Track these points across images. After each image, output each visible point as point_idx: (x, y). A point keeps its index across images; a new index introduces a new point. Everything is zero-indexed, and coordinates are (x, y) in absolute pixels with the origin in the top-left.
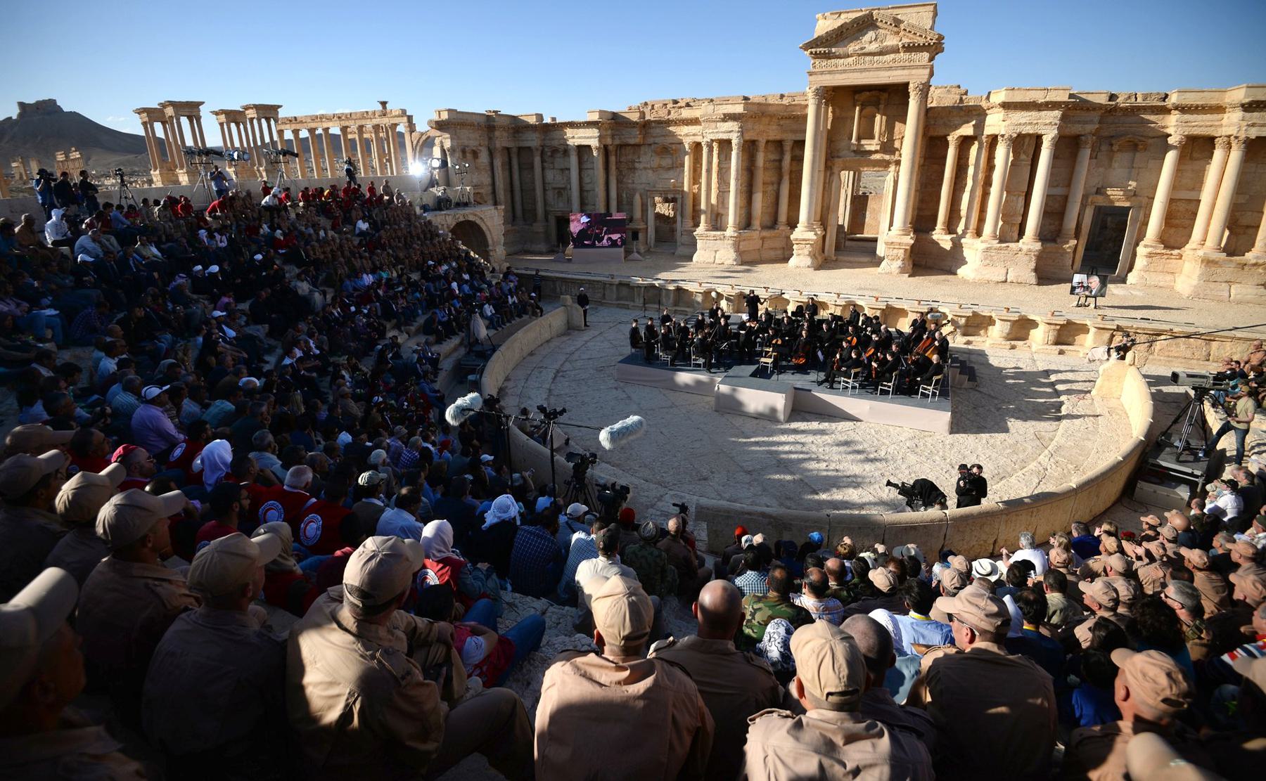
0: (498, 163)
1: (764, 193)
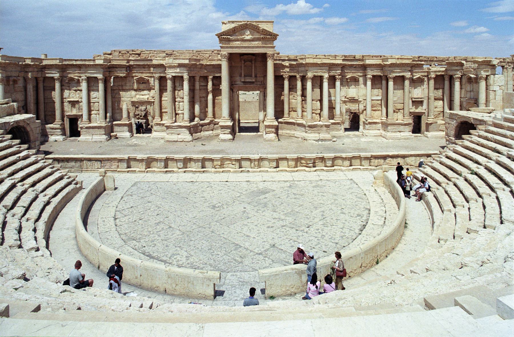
0: (30, 87)
1: (200, 101)
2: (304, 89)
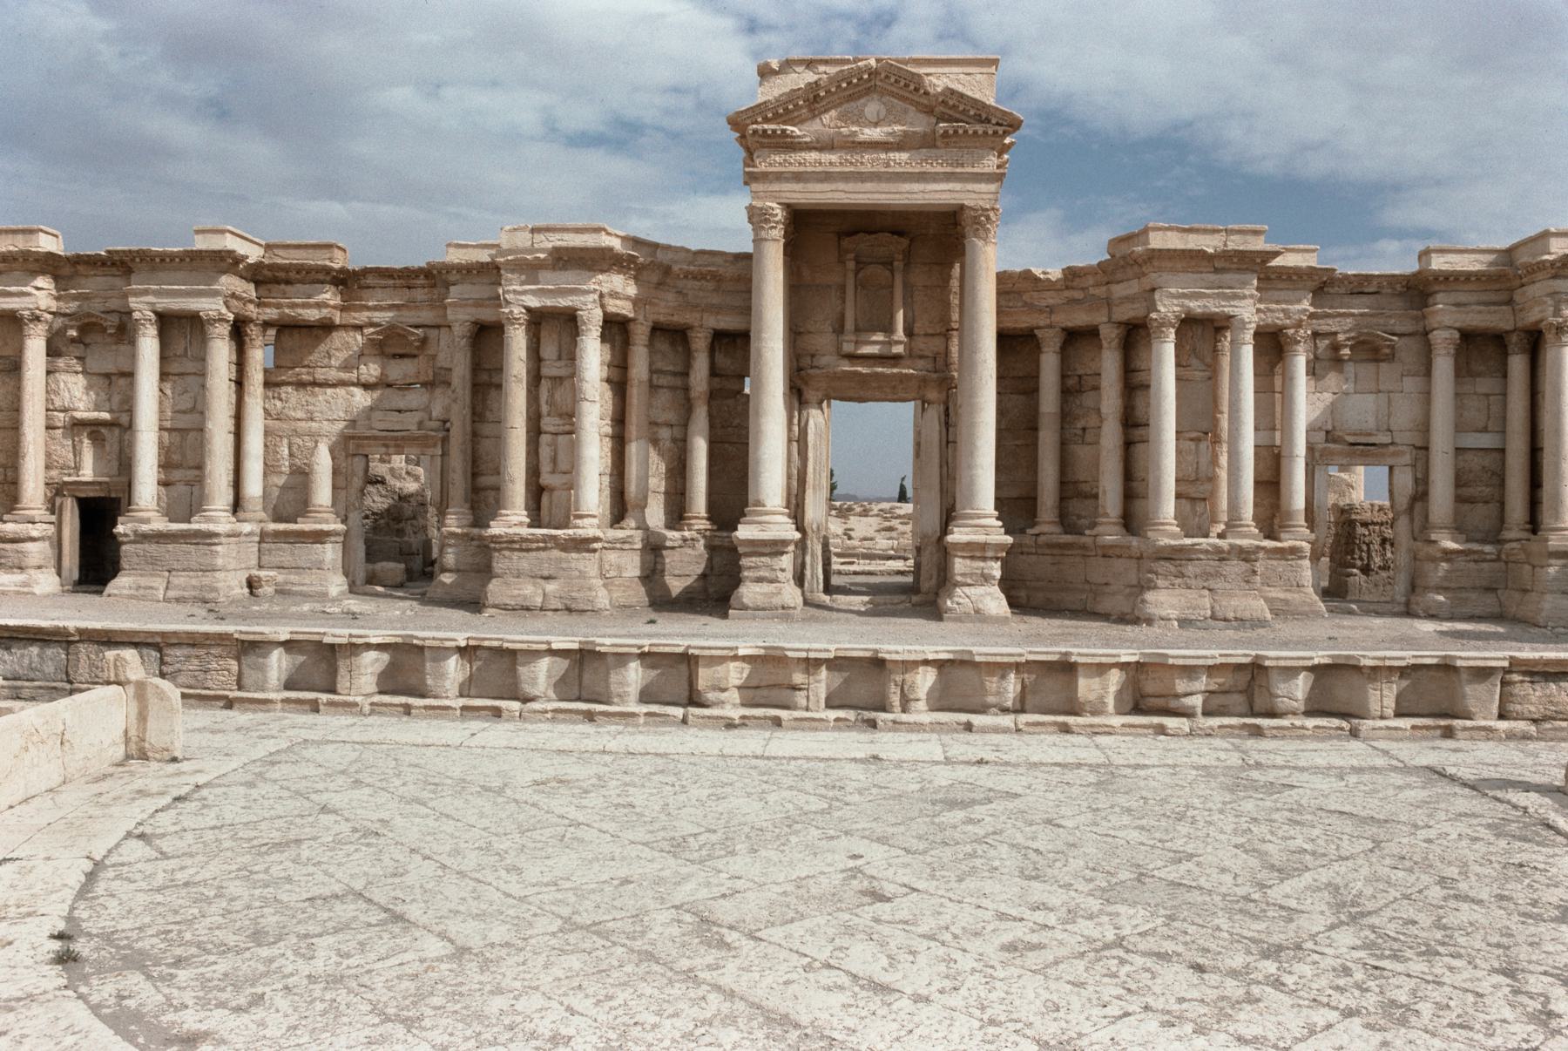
2: (1135, 385)
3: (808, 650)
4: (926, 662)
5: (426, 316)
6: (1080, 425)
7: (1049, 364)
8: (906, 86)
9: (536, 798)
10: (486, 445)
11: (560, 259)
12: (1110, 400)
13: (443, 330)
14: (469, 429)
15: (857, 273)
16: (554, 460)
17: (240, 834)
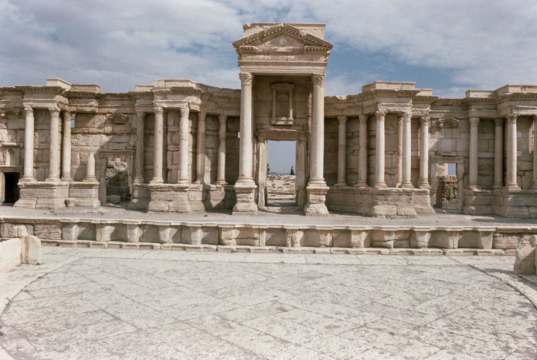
2: (371, 136)
3: (259, 226)
4: (300, 230)
5: (128, 110)
6: (353, 149)
7: (342, 128)
8: (294, 33)
9: (165, 277)
10: (149, 155)
11: (175, 91)
12: (362, 141)
13: (134, 115)
14: (143, 149)
15: (277, 96)
16: (172, 160)
17: (62, 290)
